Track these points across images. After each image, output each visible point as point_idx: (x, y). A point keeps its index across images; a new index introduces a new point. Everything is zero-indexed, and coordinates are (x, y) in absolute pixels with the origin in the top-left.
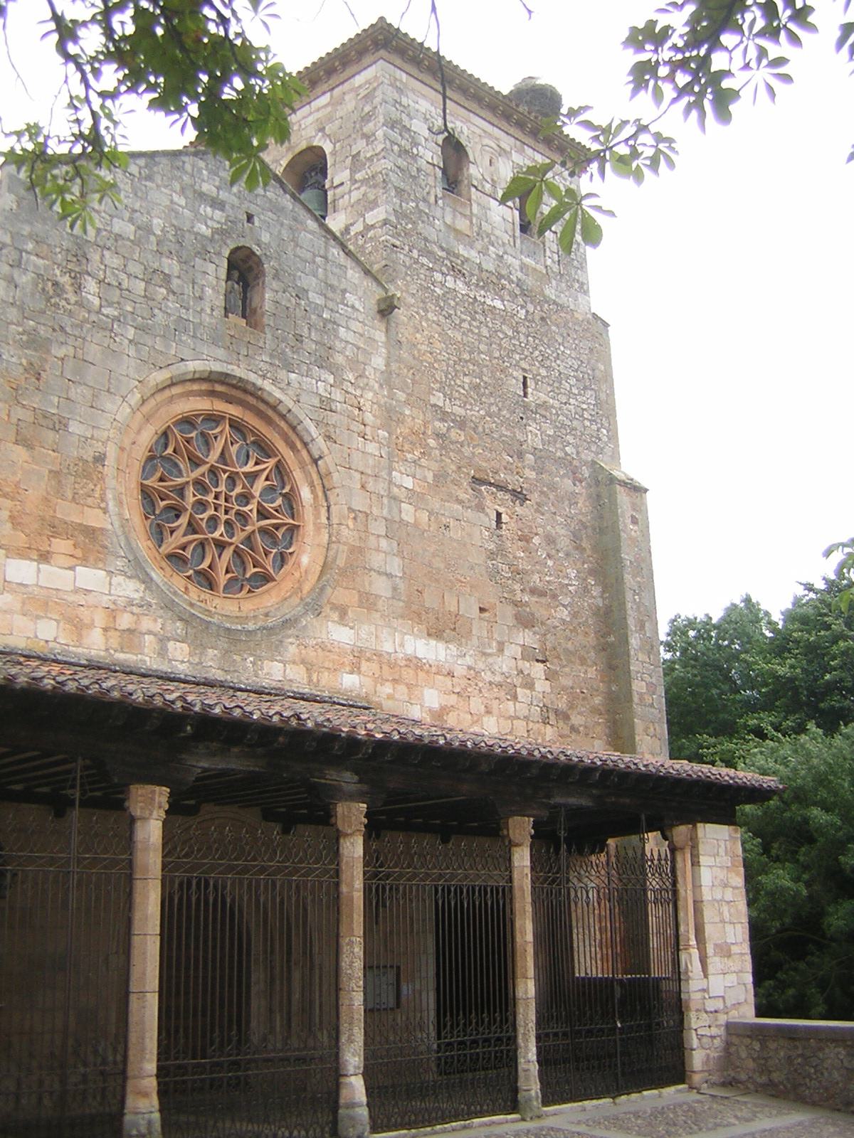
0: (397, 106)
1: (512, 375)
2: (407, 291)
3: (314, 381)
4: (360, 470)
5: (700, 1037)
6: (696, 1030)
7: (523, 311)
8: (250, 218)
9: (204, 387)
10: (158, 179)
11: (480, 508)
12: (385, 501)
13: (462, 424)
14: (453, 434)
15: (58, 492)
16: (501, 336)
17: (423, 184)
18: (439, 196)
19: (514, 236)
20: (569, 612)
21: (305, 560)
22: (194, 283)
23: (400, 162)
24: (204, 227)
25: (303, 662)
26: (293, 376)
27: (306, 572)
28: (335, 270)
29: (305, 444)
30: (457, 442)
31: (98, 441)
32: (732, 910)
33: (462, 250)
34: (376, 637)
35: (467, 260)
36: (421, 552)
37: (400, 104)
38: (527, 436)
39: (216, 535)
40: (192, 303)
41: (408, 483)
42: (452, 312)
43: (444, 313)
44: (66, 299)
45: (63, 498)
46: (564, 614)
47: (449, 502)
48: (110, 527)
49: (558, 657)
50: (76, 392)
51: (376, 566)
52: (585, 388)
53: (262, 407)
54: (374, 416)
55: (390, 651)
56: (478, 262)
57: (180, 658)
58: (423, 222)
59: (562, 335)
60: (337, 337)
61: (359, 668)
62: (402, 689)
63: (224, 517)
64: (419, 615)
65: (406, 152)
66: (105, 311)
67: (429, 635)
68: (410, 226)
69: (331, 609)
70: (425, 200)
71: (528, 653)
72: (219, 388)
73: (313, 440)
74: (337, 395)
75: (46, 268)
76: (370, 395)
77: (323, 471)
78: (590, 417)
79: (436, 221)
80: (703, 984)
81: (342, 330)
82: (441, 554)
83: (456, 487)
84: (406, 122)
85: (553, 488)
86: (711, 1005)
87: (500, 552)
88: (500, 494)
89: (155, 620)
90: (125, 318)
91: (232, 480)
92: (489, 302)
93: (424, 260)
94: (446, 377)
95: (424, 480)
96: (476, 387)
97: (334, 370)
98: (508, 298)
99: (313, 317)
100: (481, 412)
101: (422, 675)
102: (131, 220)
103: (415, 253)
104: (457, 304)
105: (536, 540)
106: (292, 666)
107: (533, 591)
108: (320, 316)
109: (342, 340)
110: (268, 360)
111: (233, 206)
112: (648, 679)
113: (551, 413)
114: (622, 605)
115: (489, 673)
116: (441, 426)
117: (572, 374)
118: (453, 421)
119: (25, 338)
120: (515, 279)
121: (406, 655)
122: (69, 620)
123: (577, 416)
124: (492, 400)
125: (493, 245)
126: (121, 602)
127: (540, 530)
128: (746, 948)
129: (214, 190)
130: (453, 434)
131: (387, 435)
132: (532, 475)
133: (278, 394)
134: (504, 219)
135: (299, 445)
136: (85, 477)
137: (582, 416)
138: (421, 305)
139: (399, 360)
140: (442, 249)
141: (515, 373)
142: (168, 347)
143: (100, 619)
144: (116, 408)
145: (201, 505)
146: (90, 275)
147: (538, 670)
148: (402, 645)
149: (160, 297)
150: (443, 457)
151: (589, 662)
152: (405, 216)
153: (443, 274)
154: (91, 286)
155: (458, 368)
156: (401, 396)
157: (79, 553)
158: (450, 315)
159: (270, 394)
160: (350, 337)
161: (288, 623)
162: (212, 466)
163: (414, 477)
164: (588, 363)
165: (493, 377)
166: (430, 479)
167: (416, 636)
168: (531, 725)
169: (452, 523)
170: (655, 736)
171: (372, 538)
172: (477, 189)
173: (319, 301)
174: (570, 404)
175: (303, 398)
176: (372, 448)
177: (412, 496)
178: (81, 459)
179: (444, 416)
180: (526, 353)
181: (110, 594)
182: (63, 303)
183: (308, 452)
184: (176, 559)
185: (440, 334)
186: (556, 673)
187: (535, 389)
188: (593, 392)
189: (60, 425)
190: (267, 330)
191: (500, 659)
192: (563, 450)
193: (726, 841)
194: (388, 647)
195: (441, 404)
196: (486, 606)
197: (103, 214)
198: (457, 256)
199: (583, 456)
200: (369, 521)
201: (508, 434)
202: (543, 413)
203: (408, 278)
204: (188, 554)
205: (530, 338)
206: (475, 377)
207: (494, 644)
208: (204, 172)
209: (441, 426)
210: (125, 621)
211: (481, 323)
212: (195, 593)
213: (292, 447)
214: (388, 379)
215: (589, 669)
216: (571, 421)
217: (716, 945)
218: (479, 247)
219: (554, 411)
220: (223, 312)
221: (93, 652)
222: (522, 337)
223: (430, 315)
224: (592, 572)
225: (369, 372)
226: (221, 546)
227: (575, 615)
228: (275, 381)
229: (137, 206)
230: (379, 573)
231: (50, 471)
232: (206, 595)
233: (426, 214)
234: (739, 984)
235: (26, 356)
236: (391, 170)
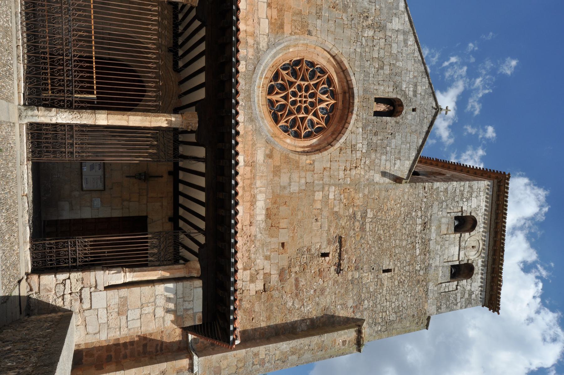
0: (478, 189)
3: (361, 141)
4: (331, 167)
5: (64, 283)
6: (69, 278)
7: (419, 269)
8: (414, 110)
9: (346, 88)
10: (416, 65)
11: (329, 243)
12: (321, 182)
13: (363, 229)
14: (357, 224)
15: (294, 13)
16: (405, 254)
17: (453, 204)
18: (451, 214)
19: (448, 262)
20: (291, 307)
21: (288, 141)
23: (458, 191)
26: (361, 130)
27: (283, 141)
28: (407, 154)
30: (354, 227)
31: (316, 32)
33: (433, 228)
34: (262, 176)
35: (430, 231)
36: (303, 204)
37: (480, 191)
38: (366, 273)
39: (290, 95)
40: (376, 79)
41: (331, 196)
42: (407, 223)
43: (406, 218)
45: (293, 15)
47: (328, 221)
48: (285, 36)
51: (293, 176)
52: (396, 313)
53: (345, 117)
54: (355, 176)
55: (257, 185)
56: (432, 238)
58: (438, 204)
60: (382, 154)
63: (299, 99)
64: (275, 203)
65: (463, 195)
66: (363, 38)
67: (267, 209)
69: (270, 149)
70: (447, 205)
71: (267, 276)
72: (347, 95)
73: (338, 141)
74: (359, 155)
76: (363, 173)
77: (327, 148)
78: (384, 317)
79: (441, 213)
80: (101, 287)
81: (384, 157)
82: (304, 216)
83: (335, 226)
84: (474, 195)
86: (86, 293)
87: (312, 257)
89: (253, 55)
90: (363, 47)
91: (312, 104)
92: (417, 246)
93: (424, 205)
94: (380, 219)
95: (335, 206)
99: (386, 141)
101: (248, 204)
102: (398, 52)
103: (425, 200)
106: (243, 126)
107: (297, 280)
109: (380, 156)
110: (364, 117)
112: (267, 360)
113: (379, 289)
115: (254, 250)
116: (358, 217)
117: (400, 303)
118: (363, 223)
119: (346, 2)
121: (257, 194)
123: (382, 307)
125: (441, 248)
126: (257, 39)
127: (326, 284)
129: (419, 92)
130: (357, 224)
131: (349, 183)
133: (352, 122)
134: (453, 256)
135: (334, 137)
136: (302, 26)
137: (383, 312)
139: (380, 190)
140: (431, 216)
141: (391, 263)
144: (330, 41)
145: (300, 88)
146: (375, 32)
147: (259, 286)
148: (261, 192)
149: (374, 64)
150: (346, 218)
152: (438, 194)
153: (421, 216)
154: (370, 33)
155: (385, 226)
156: (366, 192)
157: (273, 21)
158: (406, 221)
159: (351, 118)
160: (383, 162)
162: (317, 93)
163: (335, 199)
164: (408, 315)
166: (336, 209)
167: (265, 201)
169: (319, 223)
171: (304, 173)
172: (460, 238)
174: (386, 302)
175: (353, 136)
176: (342, 174)
177: (326, 198)
179: (364, 217)
180: (402, 270)
181: (260, 34)
182: (362, 20)
184: (276, 76)
185: (396, 215)
186: (260, 299)
188: (395, 318)
189: (319, 17)
190: (375, 117)
191: (262, 258)
193: (193, 309)
194: (258, 183)
196: (285, 247)
197: (397, 39)
198: (430, 226)
199: (365, 313)
200: (311, 172)
201: (365, 260)
202: (379, 284)
204: (280, 82)
206: (384, 238)
207: (269, 253)
209: (358, 217)
211: (407, 240)
213: (333, 134)
214: (371, 183)
216: (379, 303)
217: (126, 298)
219: (381, 291)
222: (407, 268)
226: (286, 98)
227: (290, 311)
228: (356, 120)
230: (290, 178)
231: (301, 10)
232: (266, 89)
233: (442, 206)
236: (453, 186)
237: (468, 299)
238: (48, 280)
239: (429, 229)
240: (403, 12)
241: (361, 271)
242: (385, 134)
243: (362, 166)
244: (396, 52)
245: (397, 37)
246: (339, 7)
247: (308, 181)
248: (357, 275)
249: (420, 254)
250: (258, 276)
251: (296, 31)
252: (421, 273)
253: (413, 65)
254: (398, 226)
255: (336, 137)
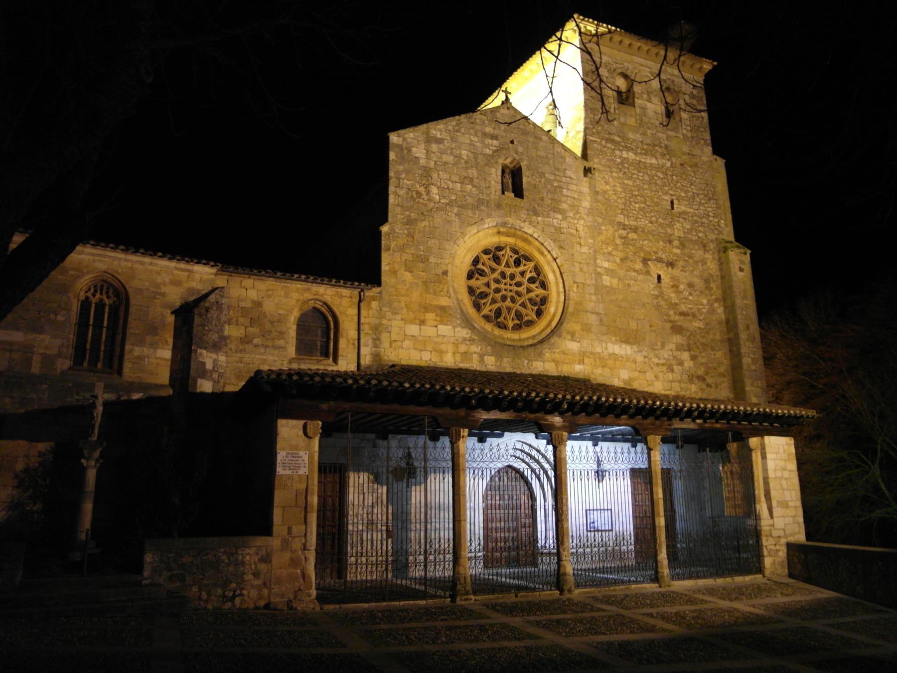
1: (664, 199)
2: (600, 164)
4: (579, 261)
8: (512, 142)
10: (463, 130)
12: (593, 275)
13: (635, 230)
16: (656, 178)
21: (552, 310)
22: (485, 179)
24: (488, 150)
25: (554, 361)
26: (540, 219)
29: (549, 252)
32: (789, 483)
41: (606, 265)
42: (626, 170)
44: (423, 199)
45: (429, 293)
46: (701, 325)
49: (698, 348)
50: (431, 242)
51: (590, 309)
52: (710, 199)
53: (525, 236)
57: (491, 364)
59: (694, 172)
61: (583, 362)
62: (607, 370)
67: (622, 342)
68: (600, 128)
71: (680, 348)
74: (564, 224)
75: (412, 185)
76: (582, 222)
80: (771, 522)
81: (565, 191)
85: (690, 257)
86: (775, 533)
87: (661, 295)
88: (659, 265)
92: (648, 161)
93: (609, 145)
95: (615, 262)
96: (641, 209)
97: (563, 212)
98: (659, 156)
99: (549, 186)
100: (647, 222)
102: (451, 154)
104: (629, 165)
105: (682, 287)
108: (552, 185)
111: (502, 137)
114: (735, 318)
118: (631, 229)
120: (663, 145)
122: (436, 351)
124: (652, 214)
125: (650, 129)
126: (460, 340)
127: (684, 281)
128: (799, 503)
129: (492, 130)
131: (592, 241)
132: (678, 251)
135: (546, 252)
138: (608, 170)
141: (666, 198)
142: (474, 214)
143: (450, 348)
146: (433, 184)
147: (685, 356)
148: (606, 348)
151: (717, 349)
154: (434, 190)
155: (631, 200)
156: (600, 220)
157: (438, 318)
158: (625, 173)
161: (542, 342)
163: (609, 261)
165: (653, 201)
166: (618, 260)
167: (613, 343)
168: (682, 385)
169: (632, 282)
170: (758, 387)
171: (587, 296)
173: (552, 177)
175: (546, 229)
176: (585, 249)
177: (609, 272)
178: (436, 274)
182: (422, 200)
183: (551, 255)
185: (620, 183)
187: (679, 204)
189: (425, 260)
192: (697, 235)
194: (598, 350)
195: (622, 221)
202: (684, 216)
203: (601, 157)
205: (674, 177)
207: (659, 344)
208: (486, 122)
209: (624, 233)
210: (463, 348)
212: (497, 331)
213: (542, 254)
215: (717, 353)
218: (641, 132)
220: (501, 192)
221: (449, 364)
223: (614, 174)
224: (716, 300)
225: (581, 210)
227: (707, 324)
228: (531, 223)
229: (453, 146)
230: (592, 313)
231: (422, 282)
234: (794, 523)
235: (407, 229)
237: (698, 101)
238: (768, 562)
239: (632, 142)
240: (404, 139)
241: (673, 237)
242: (540, 186)
243: (576, 222)
244: (452, 158)
245: (434, 153)
246: (412, 231)
247: (593, 291)
248: (676, 243)
249: (656, 158)
250: (678, 357)
251: (445, 290)
252: (674, 160)
253: (463, 134)
254: (631, 183)
255: (547, 249)
